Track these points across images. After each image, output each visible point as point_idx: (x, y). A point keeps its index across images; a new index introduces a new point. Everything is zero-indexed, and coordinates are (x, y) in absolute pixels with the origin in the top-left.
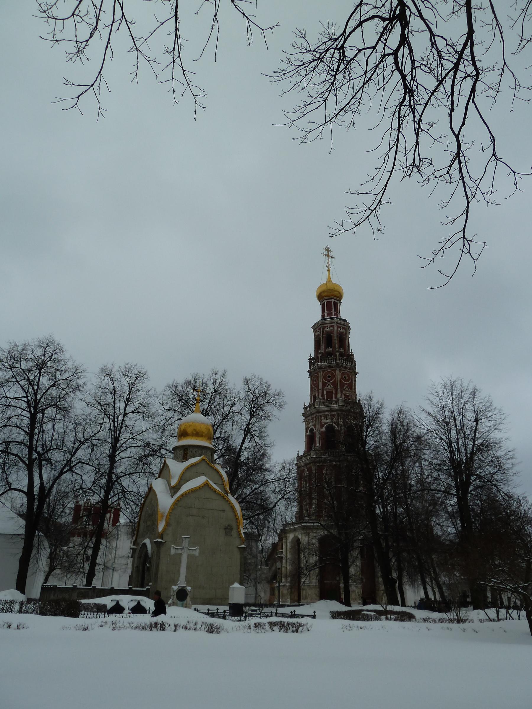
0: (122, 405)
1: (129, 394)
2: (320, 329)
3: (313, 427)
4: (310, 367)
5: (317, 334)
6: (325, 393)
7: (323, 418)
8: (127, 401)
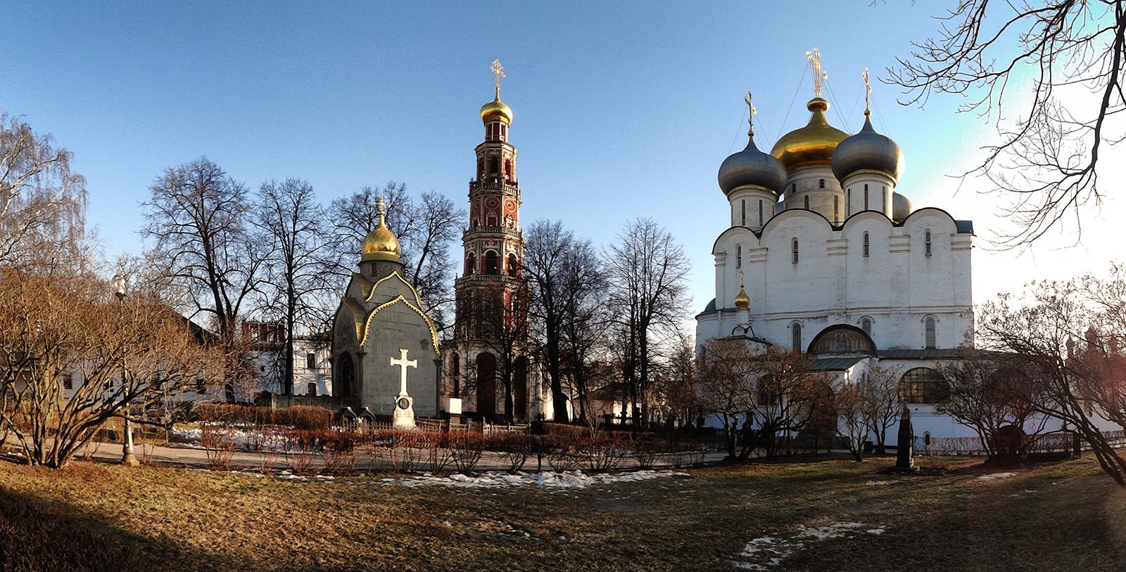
0: (290, 224)
1: (296, 212)
2: (483, 152)
3: (473, 252)
4: (471, 191)
5: (480, 157)
6: (487, 219)
7: (484, 243)
8: (295, 218)
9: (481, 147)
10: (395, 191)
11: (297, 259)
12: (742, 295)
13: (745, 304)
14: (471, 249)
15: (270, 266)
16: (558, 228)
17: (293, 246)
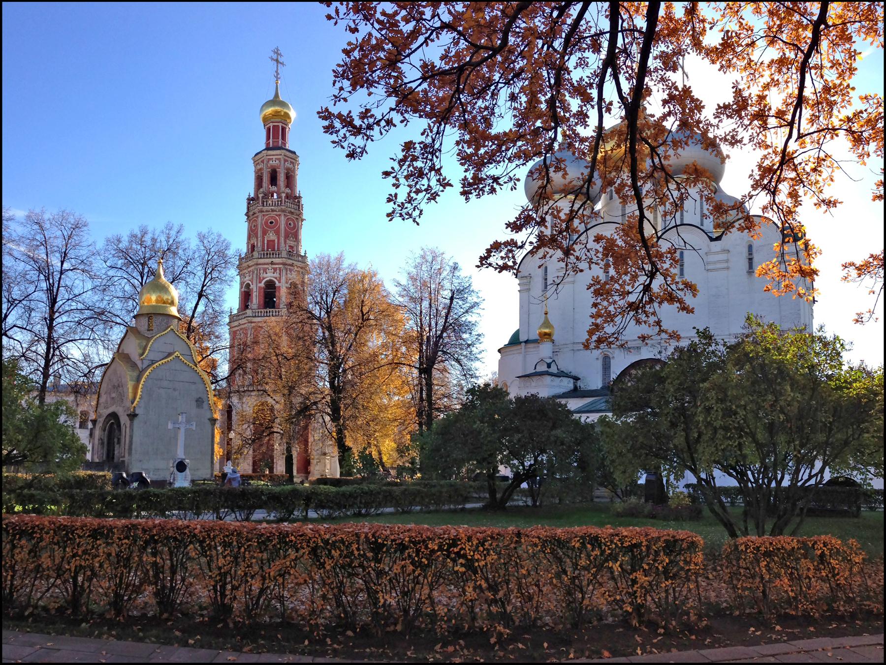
2: (263, 162)
4: (248, 208)
5: (259, 167)
9: (260, 156)
10: (173, 233)
11: (61, 303)
12: (547, 324)
13: (548, 335)
14: (247, 280)
15: (31, 310)
16: (340, 259)
17: (59, 287)
